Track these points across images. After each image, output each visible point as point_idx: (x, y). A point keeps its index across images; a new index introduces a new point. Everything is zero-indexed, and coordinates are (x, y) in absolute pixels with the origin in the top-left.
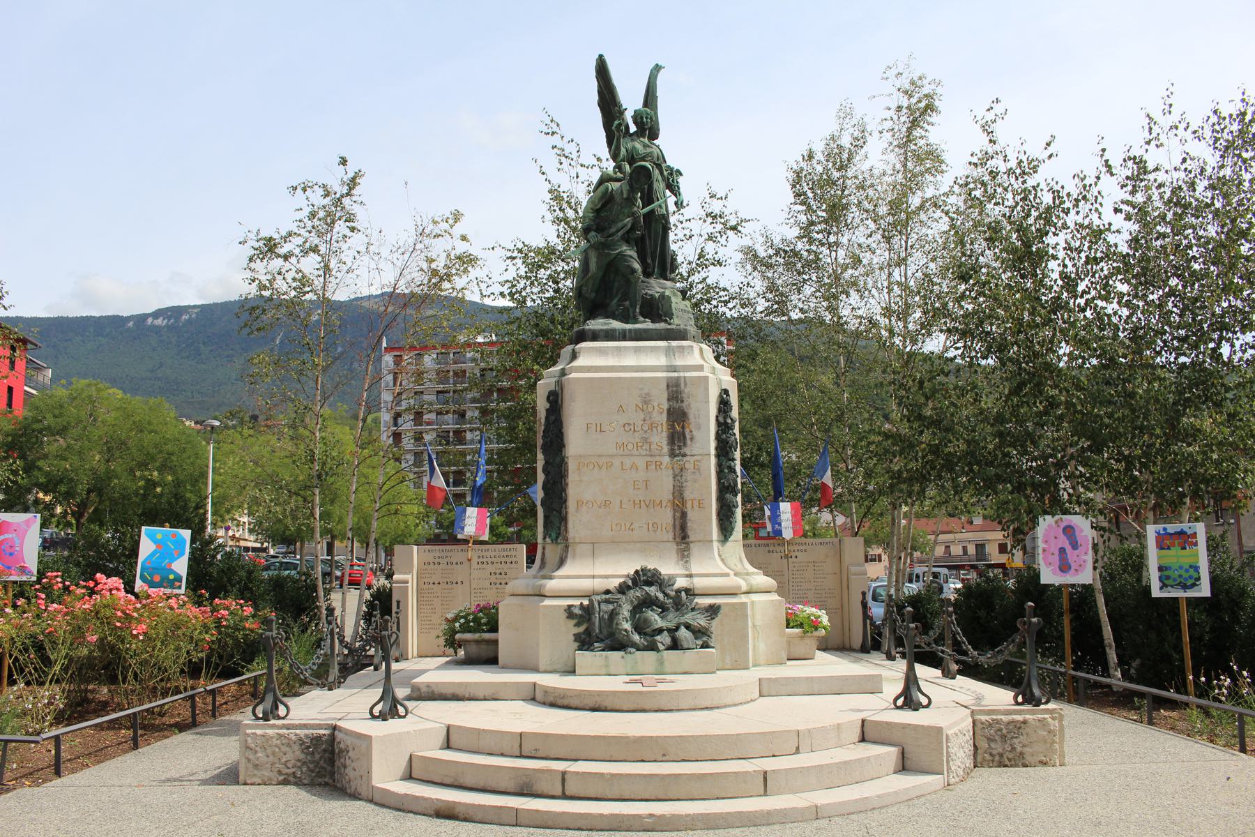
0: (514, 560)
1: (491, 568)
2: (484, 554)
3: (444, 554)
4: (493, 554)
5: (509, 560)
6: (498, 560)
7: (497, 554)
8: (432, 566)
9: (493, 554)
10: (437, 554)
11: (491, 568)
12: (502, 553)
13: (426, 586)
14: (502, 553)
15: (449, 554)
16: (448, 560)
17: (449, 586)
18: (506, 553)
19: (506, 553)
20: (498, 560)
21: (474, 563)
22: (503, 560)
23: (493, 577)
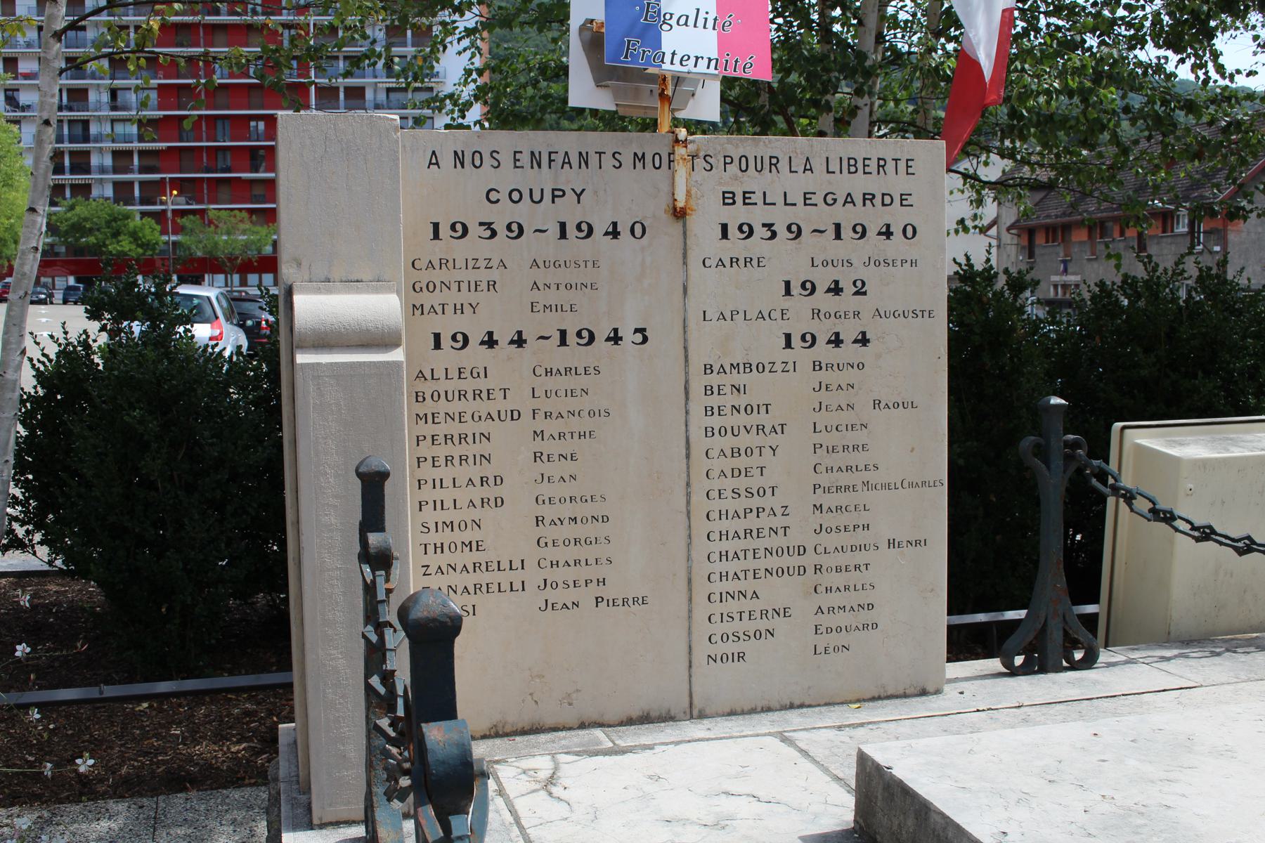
0: (897, 217)
1: (788, 260)
2: (754, 182)
3: (545, 179)
4: (796, 184)
5: (874, 218)
6: (824, 216)
7: (818, 182)
8: (475, 245)
9: (796, 184)
10: (506, 179)
11: (788, 260)
12: (845, 184)
13: (449, 357)
14: (845, 184)
15: (571, 178)
16: (569, 211)
17: (575, 354)
18: (859, 184)
19: (859, 184)
20: (824, 216)
21: (704, 225)
22: (847, 216)
23: (800, 304)
